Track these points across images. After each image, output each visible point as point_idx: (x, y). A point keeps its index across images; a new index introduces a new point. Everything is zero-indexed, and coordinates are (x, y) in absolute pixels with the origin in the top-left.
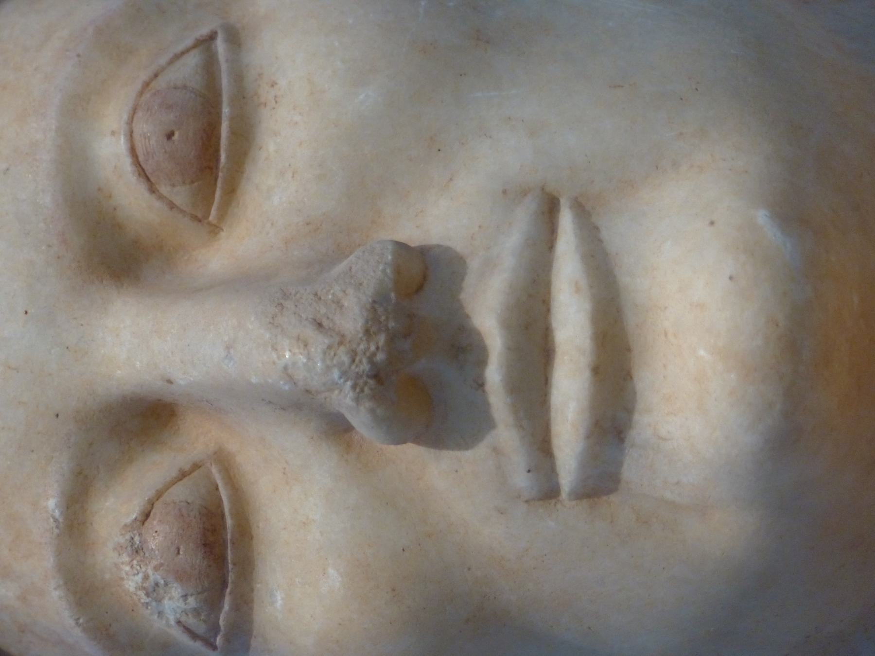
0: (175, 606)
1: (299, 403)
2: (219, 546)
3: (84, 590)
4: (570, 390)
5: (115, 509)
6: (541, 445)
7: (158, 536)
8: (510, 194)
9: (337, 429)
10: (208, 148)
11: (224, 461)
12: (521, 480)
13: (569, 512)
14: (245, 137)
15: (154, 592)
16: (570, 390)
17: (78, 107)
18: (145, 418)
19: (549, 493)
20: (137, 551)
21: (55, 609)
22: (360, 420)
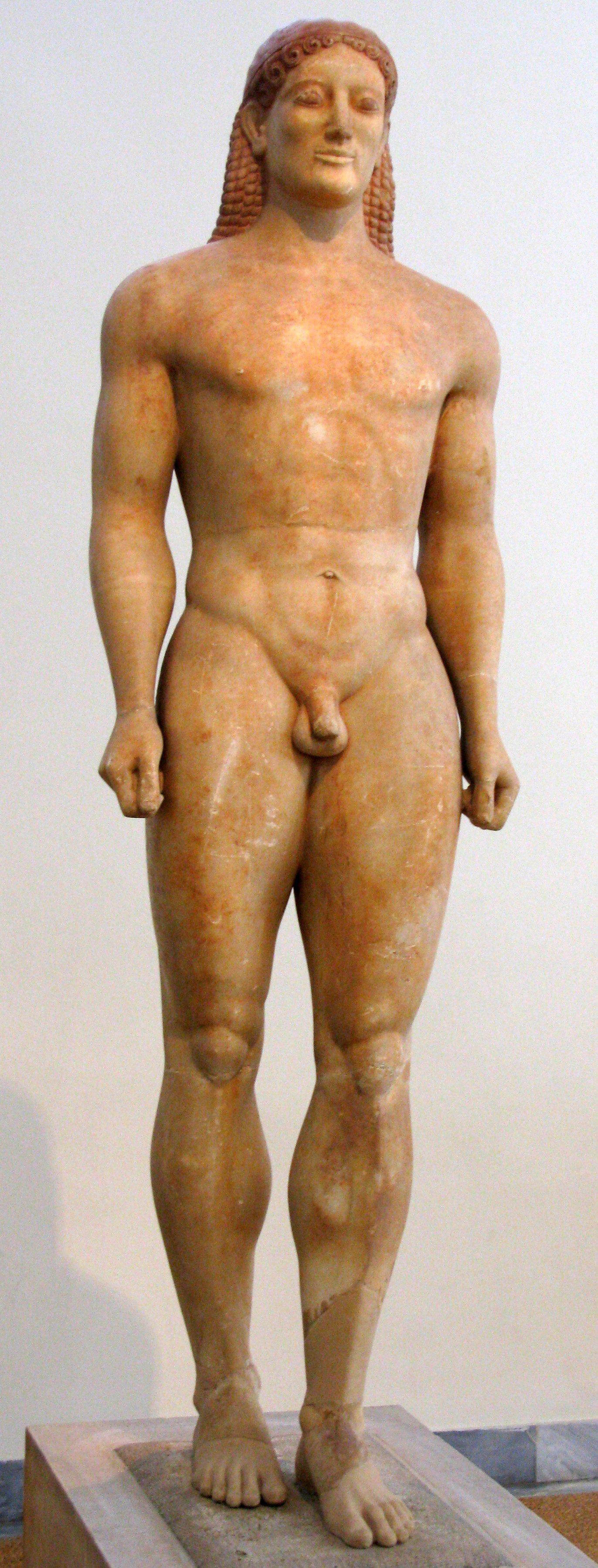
0: (304, 96)
1: (333, 120)
2: (310, 103)
3: (306, 83)
4: (332, 159)
5: (318, 90)
6: (323, 153)
7: (314, 95)
8: (356, 152)
9: (327, 124)
10: (364, 108)
11: (322, 106)
12: (318, 149)
13: (311, 155)
14: (365, 113)
15: (306, 94)
16: (332, 159)
17: (372, 91)
18: (330, 95)
19: (316, 153)
20: (312, 92)
21: (304, 78)
22: (330, 129)
